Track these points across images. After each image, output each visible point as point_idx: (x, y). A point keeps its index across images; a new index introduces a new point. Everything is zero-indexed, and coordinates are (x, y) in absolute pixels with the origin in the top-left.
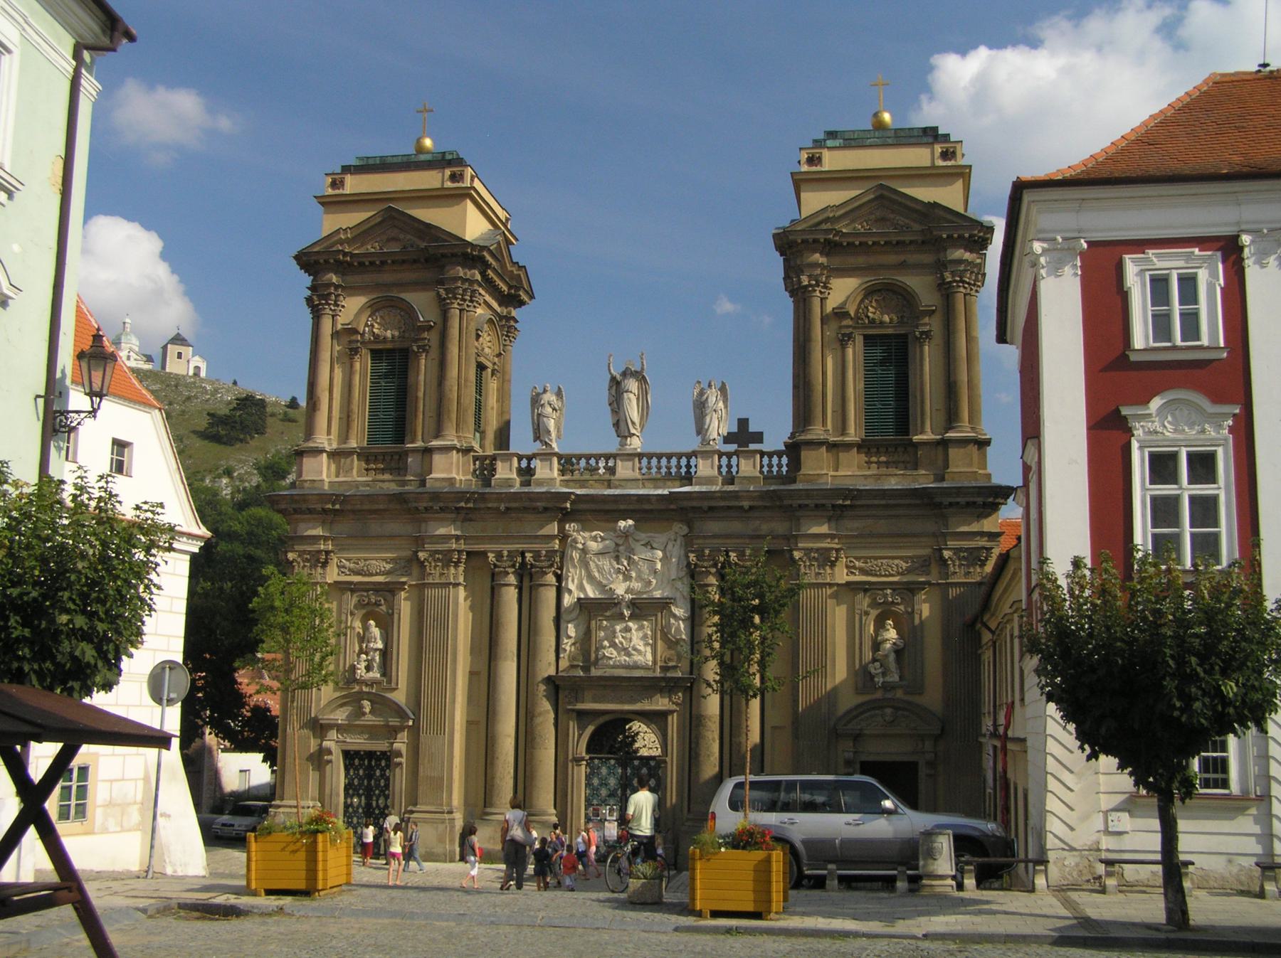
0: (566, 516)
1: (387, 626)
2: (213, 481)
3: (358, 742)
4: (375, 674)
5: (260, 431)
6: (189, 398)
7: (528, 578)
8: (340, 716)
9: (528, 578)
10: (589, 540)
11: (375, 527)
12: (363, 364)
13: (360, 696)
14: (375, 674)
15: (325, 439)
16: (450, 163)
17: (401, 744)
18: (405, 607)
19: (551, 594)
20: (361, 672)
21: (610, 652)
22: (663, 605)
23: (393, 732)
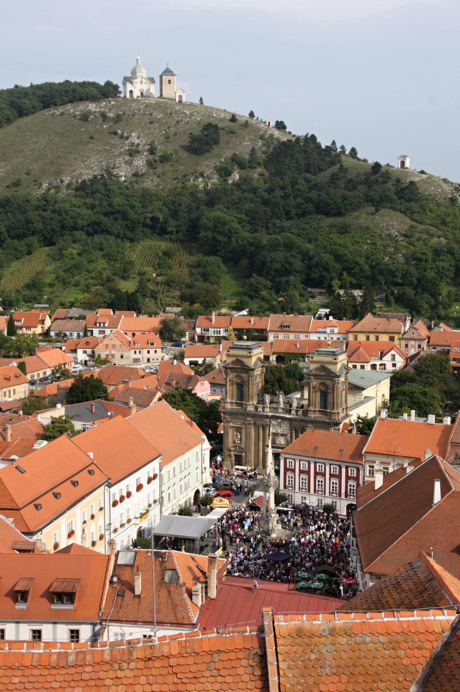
0: (270, 418)
1: (241, 433)
2: (194, 180)
3: (236, 453)
4: (239, 442)
5: (216, 142)
6: (178, 122)
7: (264, 428)
8: (233, 449)
9: (264, 428)
10: (274, 422)
11: (238, 417)
12: (235, 387)
13: (236, 446)
14: (239, 442)
15: (229, 400)
16: (249, 349)
17: (243, 454)
18: (243, 432)
19: (268, 431)
20: (237, 441)
21: (277, 442)
22: (286, 435)
23: (242, 452)
